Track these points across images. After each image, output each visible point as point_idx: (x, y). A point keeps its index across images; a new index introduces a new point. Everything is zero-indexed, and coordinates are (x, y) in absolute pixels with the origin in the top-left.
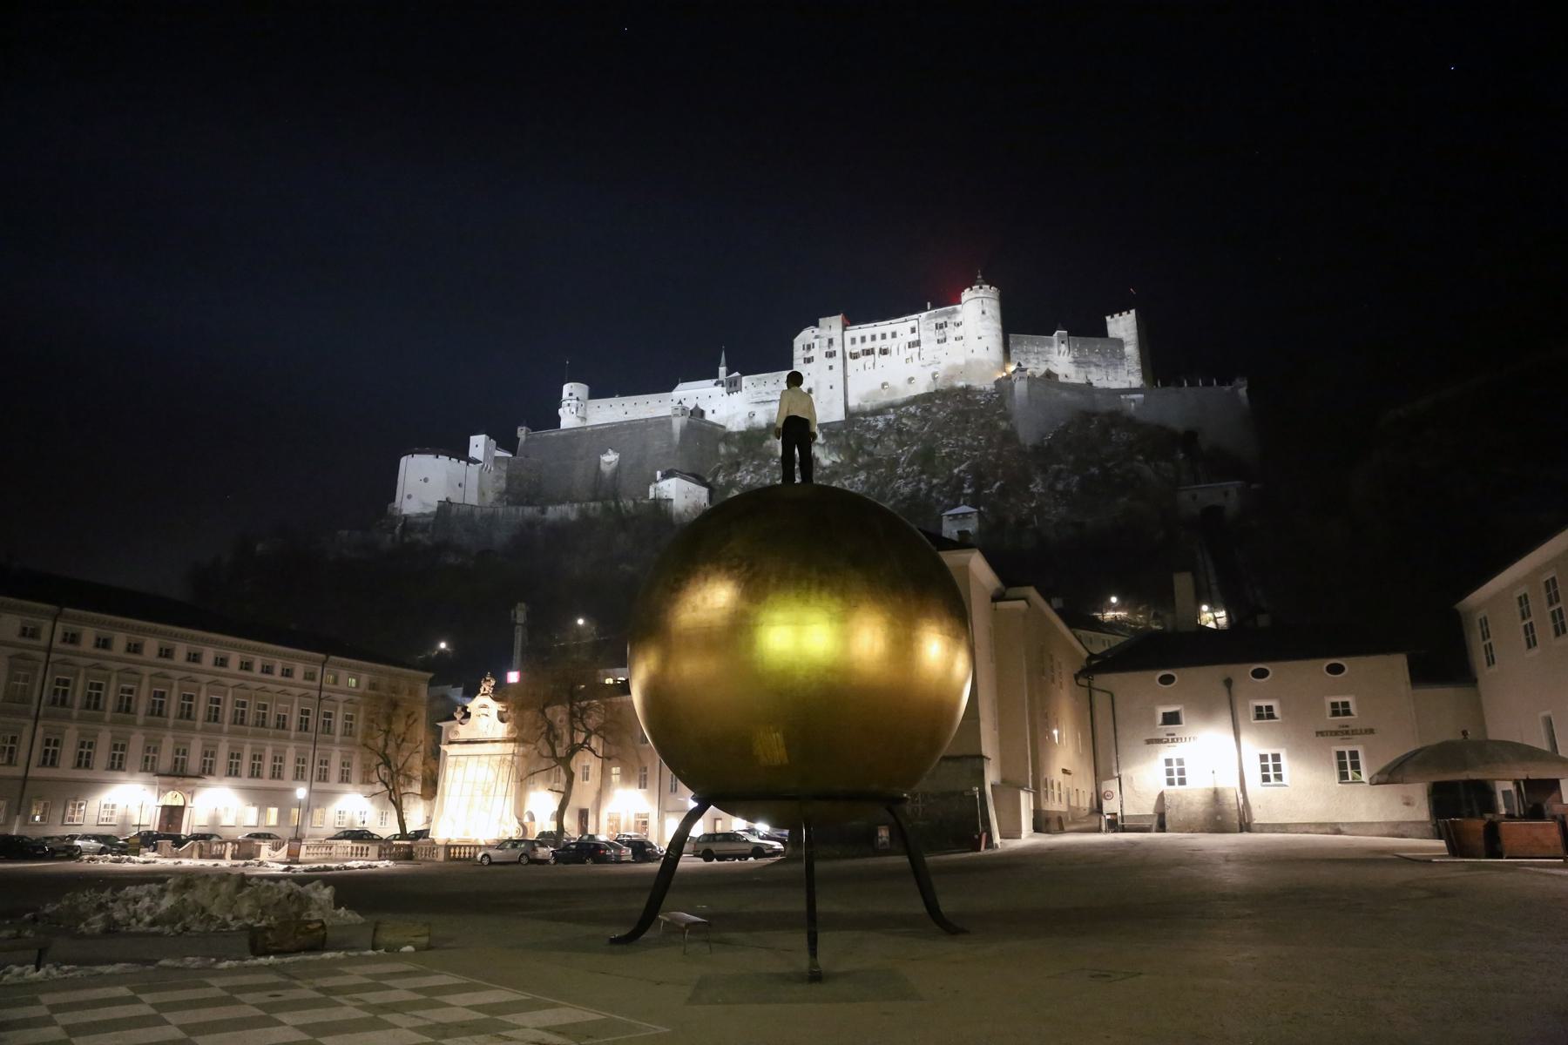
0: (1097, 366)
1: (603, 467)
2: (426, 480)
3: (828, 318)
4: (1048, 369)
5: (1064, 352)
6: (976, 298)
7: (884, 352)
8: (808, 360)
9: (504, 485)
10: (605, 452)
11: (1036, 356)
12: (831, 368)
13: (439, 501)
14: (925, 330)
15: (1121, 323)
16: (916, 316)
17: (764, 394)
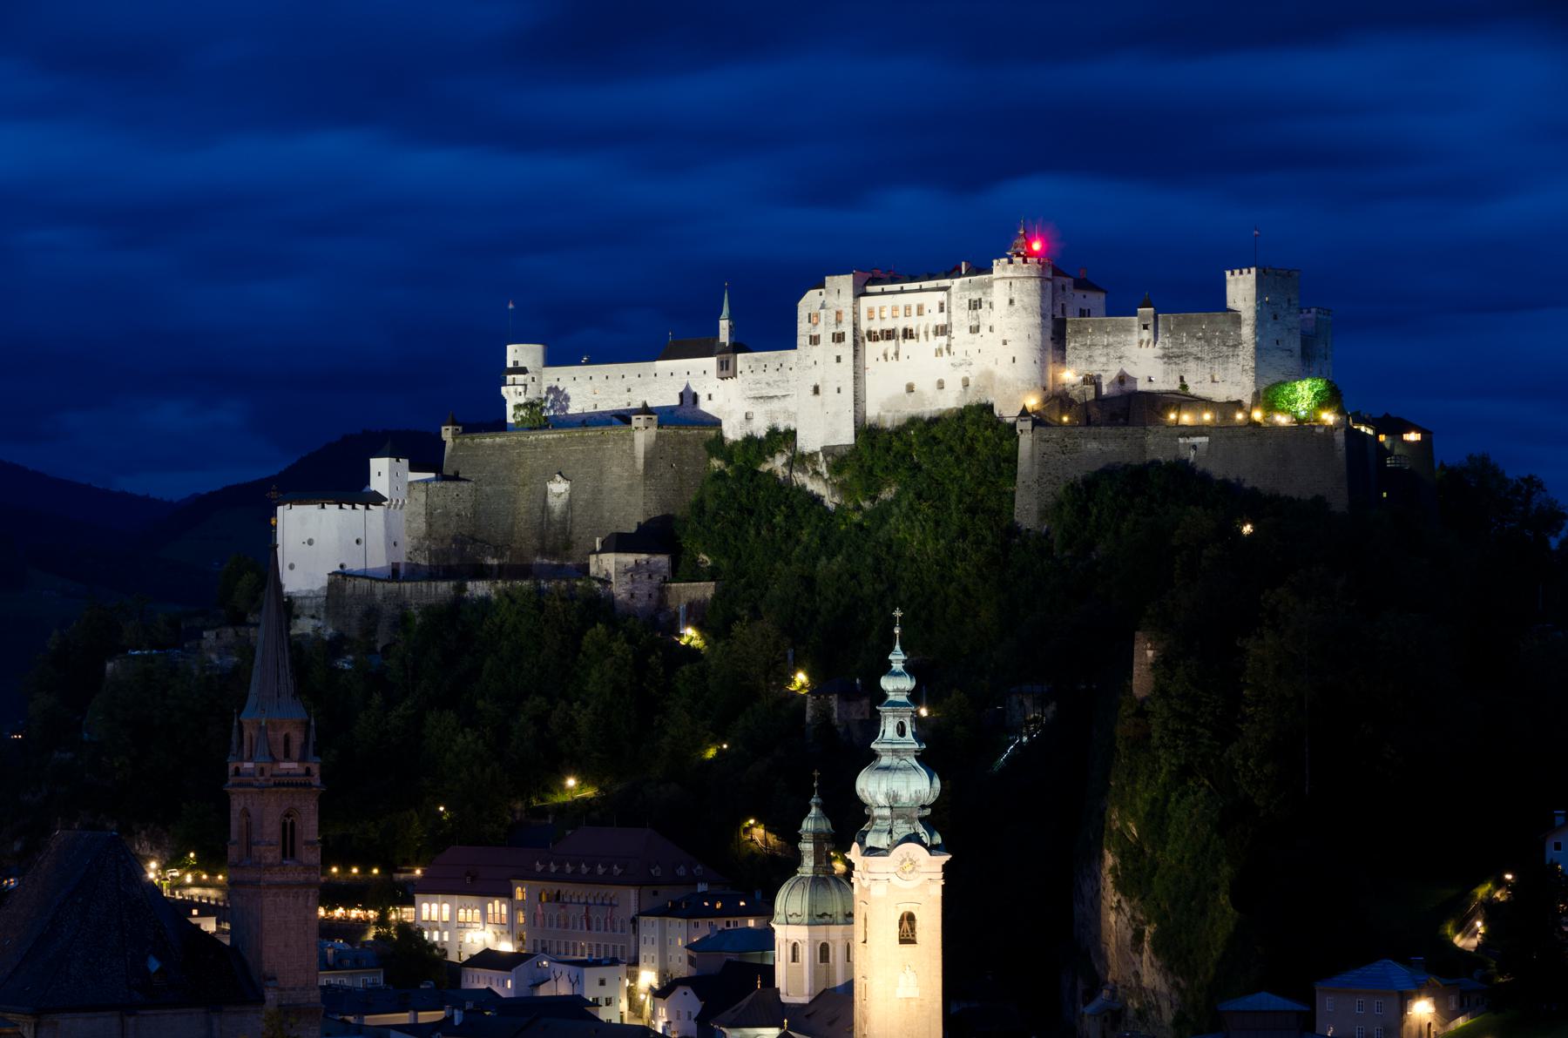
0: (1198, 358)
1: (551, 500)
2: (310, 542)
3: (836, 277)
4: (1122, 370)
5: (1148, 343)
6: (1004, 278)
7: (908, 334)
8: (815, 340)
9: (423, 527)
10: (553, 479)
11: (1105, 351)
12: (838, 359)
13: (329, 574)
14: (958, 307)
15: (1241, 286)
16: (946, 282)
17: (763, 385)
